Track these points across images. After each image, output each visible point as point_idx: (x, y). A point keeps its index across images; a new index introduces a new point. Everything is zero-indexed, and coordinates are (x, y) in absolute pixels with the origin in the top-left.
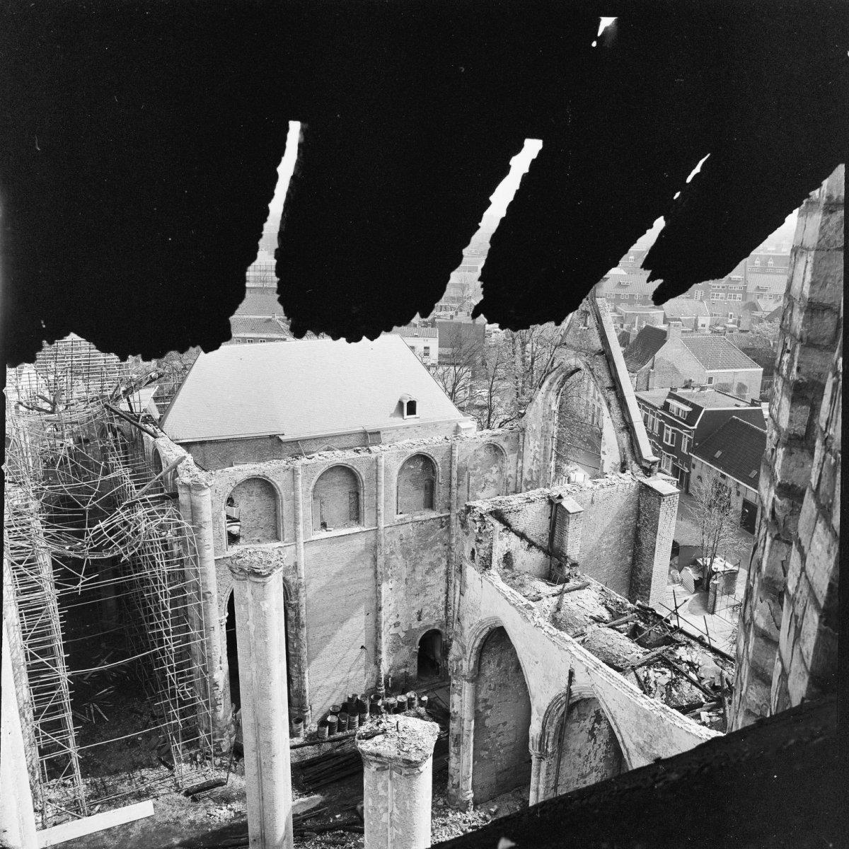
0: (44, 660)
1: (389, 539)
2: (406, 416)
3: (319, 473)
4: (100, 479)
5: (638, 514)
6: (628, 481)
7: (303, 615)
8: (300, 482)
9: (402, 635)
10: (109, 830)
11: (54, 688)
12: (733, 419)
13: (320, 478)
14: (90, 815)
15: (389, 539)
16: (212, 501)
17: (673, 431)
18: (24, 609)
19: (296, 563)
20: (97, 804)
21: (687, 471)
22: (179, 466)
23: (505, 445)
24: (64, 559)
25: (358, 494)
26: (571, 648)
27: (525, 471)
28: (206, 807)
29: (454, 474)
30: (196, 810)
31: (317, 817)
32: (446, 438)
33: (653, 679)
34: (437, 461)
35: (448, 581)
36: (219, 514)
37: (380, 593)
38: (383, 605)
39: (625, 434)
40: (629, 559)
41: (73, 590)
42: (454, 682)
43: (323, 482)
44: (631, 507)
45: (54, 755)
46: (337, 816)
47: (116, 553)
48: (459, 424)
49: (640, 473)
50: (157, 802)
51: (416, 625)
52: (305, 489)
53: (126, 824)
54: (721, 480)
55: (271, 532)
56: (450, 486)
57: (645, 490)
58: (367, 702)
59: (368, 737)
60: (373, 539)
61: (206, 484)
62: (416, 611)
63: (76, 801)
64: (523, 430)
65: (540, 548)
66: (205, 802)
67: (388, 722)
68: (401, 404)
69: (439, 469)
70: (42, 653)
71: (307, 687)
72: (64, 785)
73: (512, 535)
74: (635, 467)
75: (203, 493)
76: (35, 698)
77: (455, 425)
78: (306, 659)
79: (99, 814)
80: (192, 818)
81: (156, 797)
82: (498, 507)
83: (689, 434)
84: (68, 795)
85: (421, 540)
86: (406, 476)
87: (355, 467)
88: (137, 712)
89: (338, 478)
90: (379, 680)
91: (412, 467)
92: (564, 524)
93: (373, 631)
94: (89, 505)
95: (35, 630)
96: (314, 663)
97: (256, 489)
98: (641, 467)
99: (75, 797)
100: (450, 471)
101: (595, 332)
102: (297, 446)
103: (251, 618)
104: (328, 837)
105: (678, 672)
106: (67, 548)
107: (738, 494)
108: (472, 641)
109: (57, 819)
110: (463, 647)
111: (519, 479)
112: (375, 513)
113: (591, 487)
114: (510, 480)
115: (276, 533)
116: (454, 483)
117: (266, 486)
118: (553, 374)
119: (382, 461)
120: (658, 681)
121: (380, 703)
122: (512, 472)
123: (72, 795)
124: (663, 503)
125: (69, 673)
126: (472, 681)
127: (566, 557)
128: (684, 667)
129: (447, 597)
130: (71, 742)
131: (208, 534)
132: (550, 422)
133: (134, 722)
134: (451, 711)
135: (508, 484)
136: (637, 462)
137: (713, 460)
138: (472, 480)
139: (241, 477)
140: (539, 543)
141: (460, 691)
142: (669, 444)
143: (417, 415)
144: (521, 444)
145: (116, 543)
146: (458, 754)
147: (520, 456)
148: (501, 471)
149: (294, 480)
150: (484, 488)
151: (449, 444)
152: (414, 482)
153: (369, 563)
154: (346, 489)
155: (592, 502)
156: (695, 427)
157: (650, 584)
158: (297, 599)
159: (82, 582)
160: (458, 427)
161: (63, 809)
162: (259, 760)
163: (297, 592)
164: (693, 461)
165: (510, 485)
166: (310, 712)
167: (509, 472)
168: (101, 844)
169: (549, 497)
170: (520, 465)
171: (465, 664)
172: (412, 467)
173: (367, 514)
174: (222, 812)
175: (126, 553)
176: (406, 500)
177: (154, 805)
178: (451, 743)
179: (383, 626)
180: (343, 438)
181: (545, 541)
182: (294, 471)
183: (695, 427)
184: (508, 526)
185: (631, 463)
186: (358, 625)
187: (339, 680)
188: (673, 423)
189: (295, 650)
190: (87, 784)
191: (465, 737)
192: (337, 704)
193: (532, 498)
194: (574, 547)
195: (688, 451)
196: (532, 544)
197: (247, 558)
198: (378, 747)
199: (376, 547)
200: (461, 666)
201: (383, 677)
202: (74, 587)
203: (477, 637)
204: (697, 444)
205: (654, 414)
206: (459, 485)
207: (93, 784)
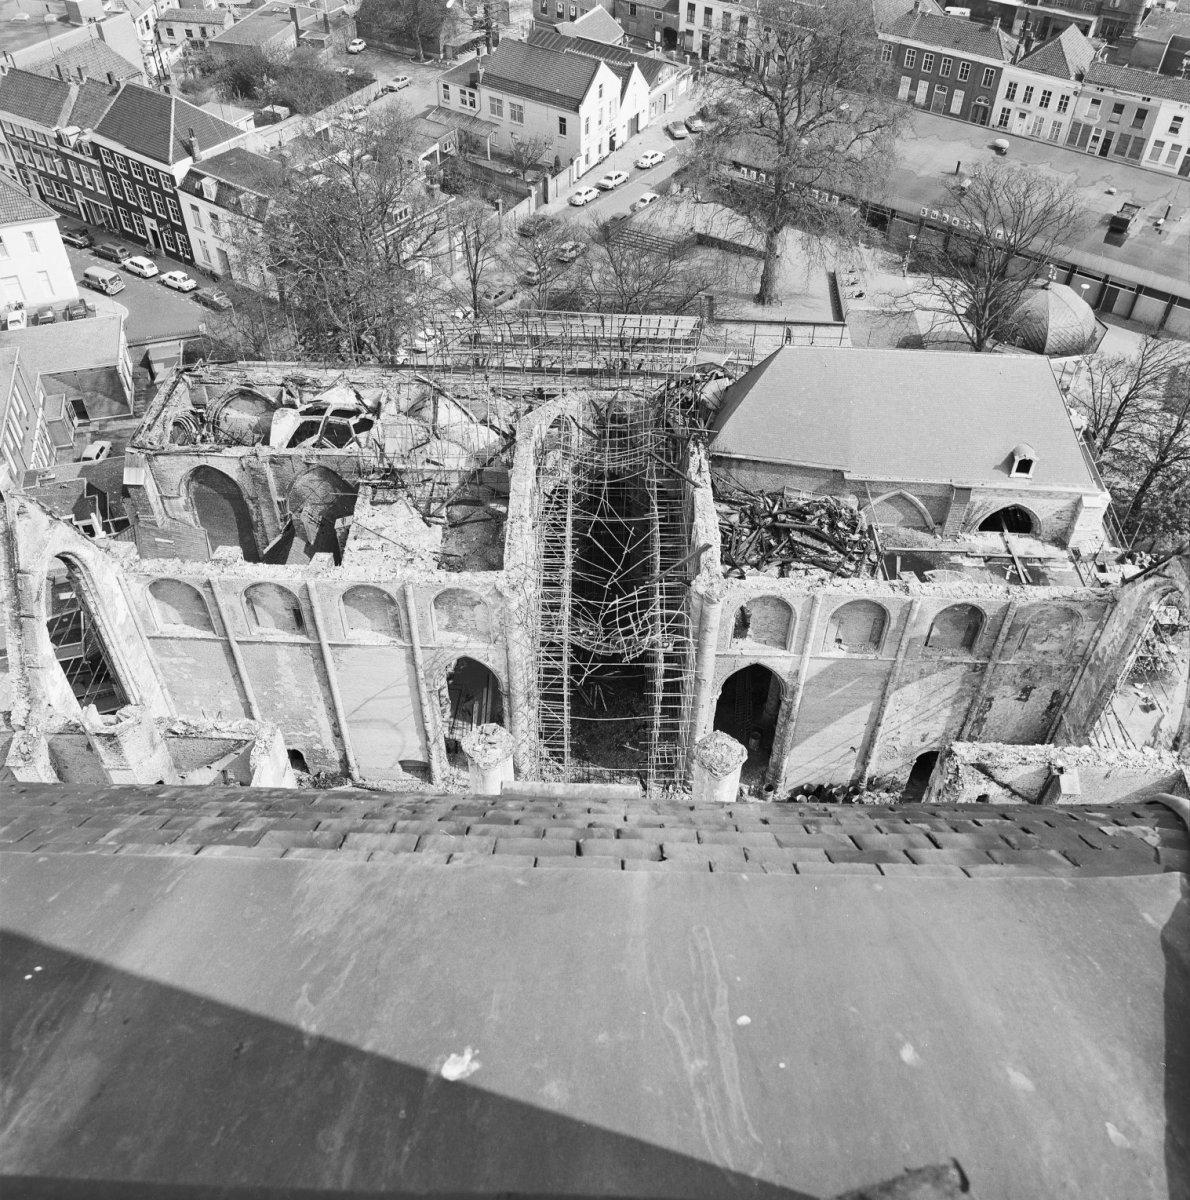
2: (1014, 473)
3: (842, 604)
7: (795, 710)
8: (817, 610)
22: (703, 556)
23: (1084, 612)
29: (1005, 630)
35: (966, 717)
36: (728, 620)
47: (620, 652)
52: (822, 614)
56: (997, 638)
64: (1115, 602)
71: (785, 766)
73: (993, 784)
75: (713, 606)
76: (545, 679)
82: (983, 761)
93: (868, 738)
96: (797, 748)
111: (1091, 647)
113: (1111, 761)
116: (1002, 637)
117: (784, 606)
118: (1162, 580)
119: (917, 607)
122: (1085, 638)
129: (962, 730)
131: (712, 639)
135: (1075, 647)
143: (1030, 475)
147: (1101, 627)
152: (956, 623)
153: (878, 685)
154: (872, 616)
155: (1107, 776)
163: (793, 693)
169: (1050, 763)
170: (1097, 634)
173: (888, 647)
179: (878, 738)
184: (991, 777)
186: (852, 727)
196: (1014, 793)
199: (889, 674)
201: (867, 776)
206: (1008, 639)
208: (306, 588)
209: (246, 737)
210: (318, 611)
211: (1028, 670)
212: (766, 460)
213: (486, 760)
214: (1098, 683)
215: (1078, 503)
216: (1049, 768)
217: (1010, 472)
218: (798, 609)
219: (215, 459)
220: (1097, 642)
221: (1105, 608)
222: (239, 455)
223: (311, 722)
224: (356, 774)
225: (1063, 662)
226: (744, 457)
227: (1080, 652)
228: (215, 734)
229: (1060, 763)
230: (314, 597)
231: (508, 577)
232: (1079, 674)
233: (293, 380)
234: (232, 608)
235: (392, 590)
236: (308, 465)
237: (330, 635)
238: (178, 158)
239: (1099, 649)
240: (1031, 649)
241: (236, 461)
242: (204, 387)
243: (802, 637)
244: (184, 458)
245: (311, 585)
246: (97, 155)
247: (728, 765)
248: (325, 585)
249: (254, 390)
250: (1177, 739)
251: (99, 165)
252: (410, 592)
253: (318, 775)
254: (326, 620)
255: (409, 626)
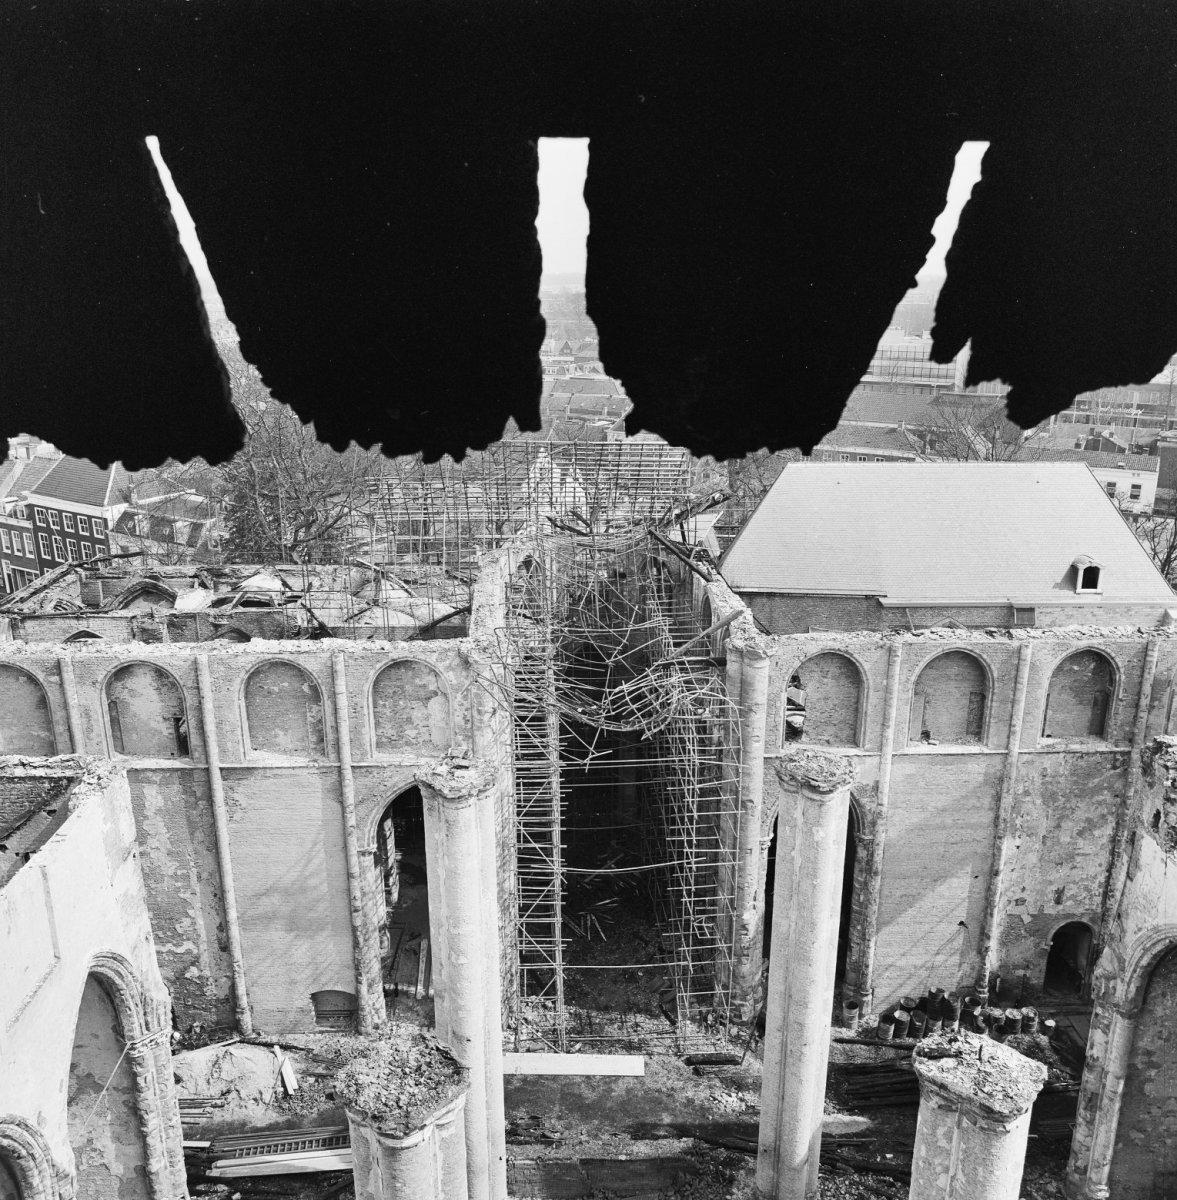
0: (537, 846)
1: (1023, 771)
2: (1079, 589)
3: (928, 659)
4: (630, 628)
7: (878, 857)
8: (897, 669)
9: (1027, 919)
10: (588, 1077)
11: (546, 883)
13: (929, 666)
14: (568, 1052)
15: (1023, 771)
16: (770, 677)
18: (524, 778)
19: (877, 782)
20: (577, 1042)
22: (732, 623)
24: (576, 725)
25: (983, 697)
28: (710, 1087)
29: (1147, 689)
30: (697, 1085)
31: (860, 1147)
32: (1139, 631)
34: (1120, 664)
35: (1113, 853)
36: (778, 695)
37: (999, 849)
38: (1001, 867)
41: (578, 765)
42: (1099, 1010)
43: (932, 673)
45: (535, 966)
46: (889, 1156)
47: (636, 727)
50: (649, 1061)
51: (1051, 909)
52: (903, 678)
53: (609, 1077)
55: (847, 732)
56: (1137, 706)
58: (958, 1005)
59: (935, 1055)
60: (999, 767)
61: (765, 653)
62: (1054, 888)
63: (555, 1030)
66: (710, 1079)
67: (967, 1042)
68: (1074, 569)
69: (1121, 677)
70: (538, 837)
71: (871, 962)
72: (545, 1007)
75: (759, 664)
76: (524, 891)
78: (874, 922)
79: (580, 1055)
80: (690, 1094)
81: (650, 1055)
84: (547, 1020)
85: (1076, 782)
86: (1066, 681)
87: (985, 656)
88: (641, 939)
89: (954, 669)
90: (980, 978)
91: (1076, 668)
93: (983, 903)
94: (612, 659)
95: (531, 807)
96: (886, 930)
97: (833, 668)
99: (554, 1025)
100: (1141, 683)
102: (904, 615)
103: (797, 848)
104: (870, 1180)
106: (580, 710)
108: (1138, 955)
109: (532, 1045)
110: (1121, 961)
112: (1007, 728)
115: (855, 735)
116: (1145, 702)
117: (849, 668)
119: (1027, 653)
121: (977, 1011)
123: (552, 1022)
125: (565, 870)
126: (1128, 1016)
129: (1109, 878)
130: (559, 956)
131: (759, 721)
133: (636, 951)
134: (1089, 1053)
139: (813, 649)
141: (1108, 1027)
143: (1098, 590)
145: (639, 714)
146: (1090, 1123)
149: (890, 664)
151: (1144, 641)
152: (1077, 691)
153: (987, 801)
154: (967, 687)
158: (873, 833)
159: (590, 756)
161: (539, 1034)
162: (784, 1045)
163: (874, 824)
166: (870, 997)
168: (576, 1091)
171: (1121, 989)
172: (1076, 668)
174: (729, 1099)
175: (649, 729)
176: (1060, 717)
177: (646, 1064)
178: (1082, 1104)
179: (997, 899)
180: (975, 612)
182: (891, 651)
186: (957, 892)
187: (919, 963)
189: (861, 904)
190: (570, 1014)
191: (1106, 1101)
192: (912, 996)
197: (802, 763)
198: (945, 1075)
199: (1001, 780)
200: (1114, 988)
201: (987, 974)
202: (580, 762)
203: (1146, 950)
206: (1151, 707)
207: (577, 1016)
208: (195, 667)
209: (69, 773)
210: (209, 706)
212: (782, 591)
213: (453, 784)
217: (1074, 587)
218: (868, 663)
219: (98, 621)
222: (131, 615)
223: (186, 922)
224: (247, 1020)
226: (756, 590)
228: (19, 772)
230: (206, 681)
231: (477, 641)
233: (208, 570)
234: (86, 713)
235: (311, 665)
236: (217, 626)
237: (223, 751)
238: (113, 503)
241: (124, 623)
242: (99, 582)
243: (880, 719)
244: (59, 622)
245: (203, 659)
246: (31, 517)
247: (833, 775)
248: (221, 661)
249: (161, 584)
251: (31, 526)
252: (340, 667)
253: (189, 1031)
254: (219, 724)
255: (336, 729)
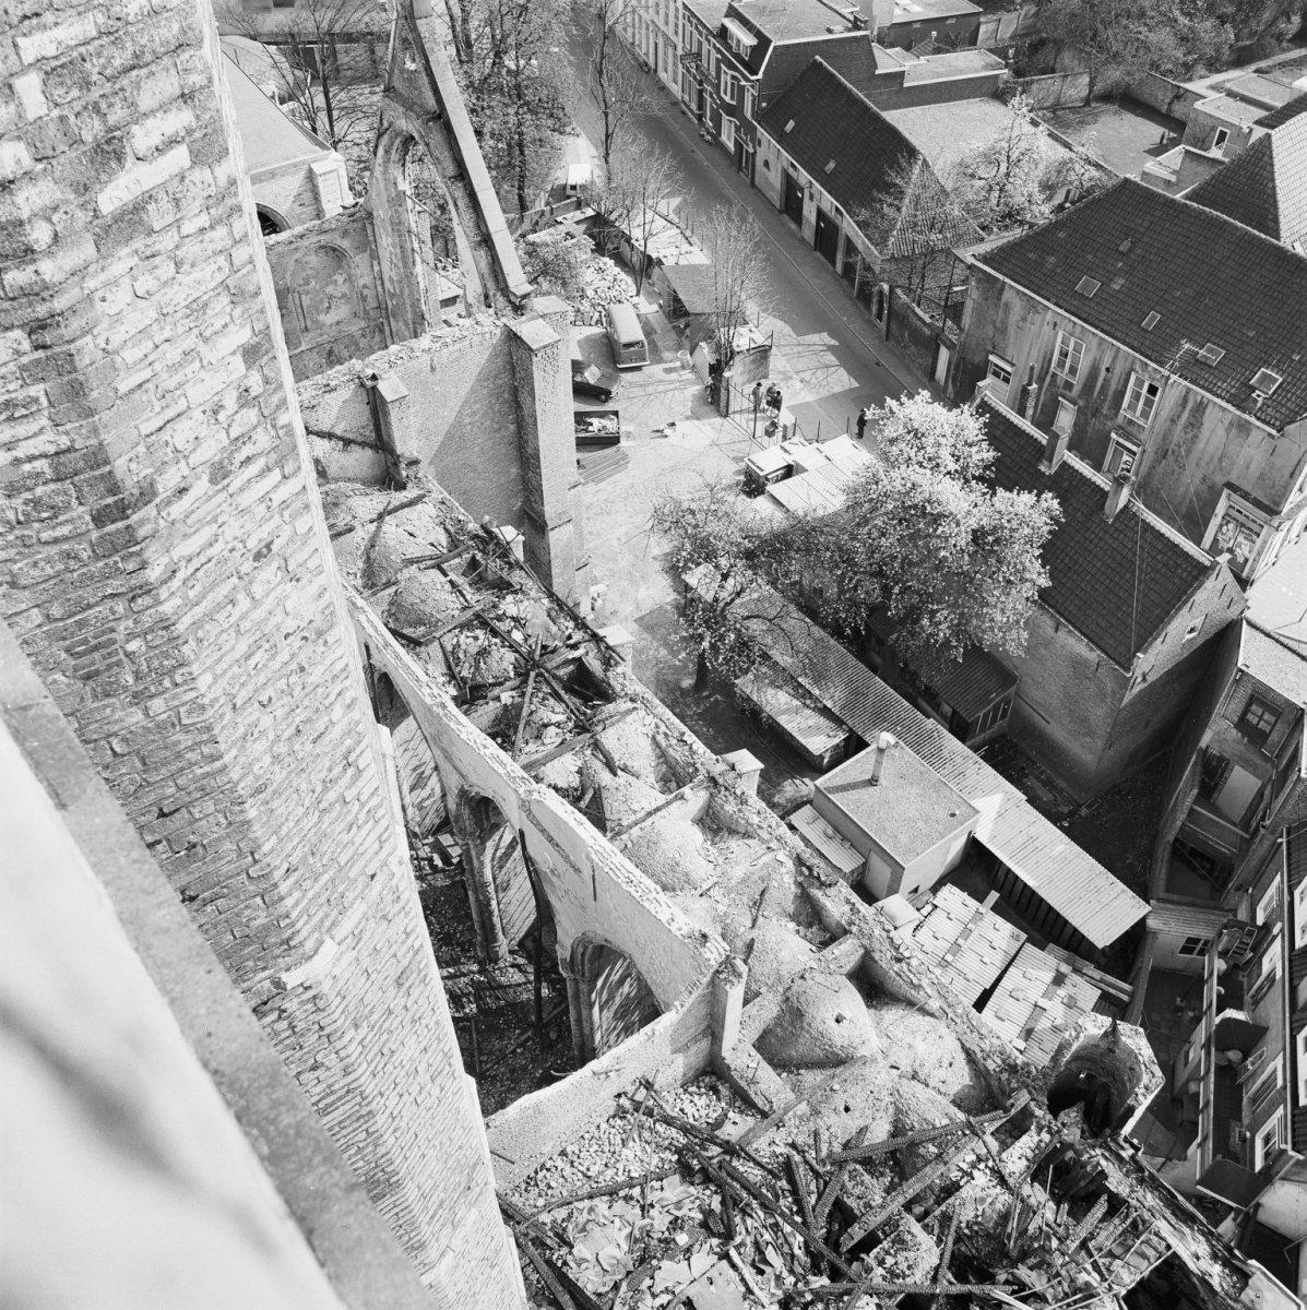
5: (512, 368)
6: (488, 326)
12: (815, 61)
17: (733, 77)
21: (751, 150)
23: (345, 244)
26: (362, 618)
27: (386, 278)
33: (463, 647)
39: (483, 252)
40: (512, 427)
44: (500, 362)
48: (313, 166)
49: (508, 311)
54: (791, 170)
57: (512, 337)
64: (370, 215)
65: (363, 444)
74: (501, 301)
77: (306, 166)
83: (753, 87)
92: (387, 414)
98: (510, 302)
101: (424, 80)
105: (495, 633)
107: (811, 197)
111: (380, 289)
114: (366, 292)
120: (470, 649)
122: (367, 280)
124: (535, 359)
127: (398, 456)
128: (503, 626)
132: (400, 210)
135: (364, 299)
136: (503, 295)
137: (782, 138)
138: (306, 301)
140: (360, 439)
142: (727, 99)
144: (371, 238)
148: (349, 280)
150: (329, 307)
155: (433, 369)
156: (760, 76)
157: (539, 461)
160: (311, 171)
164: (759, 135)
165: (369, 299)
167: (361, 282)
169: (359, 378)
170: (376, 268)
181: (370, 435)
183: (760, 76)
185: (495, 295)
188: (731, 66)
193: (333, 384)
194: (408, 440)
195: (753, 116)
204: (764, 105)
205: (709, 41)
211: (330, 353)
214: (406, 324)
215: (311, 176)
216: (362, 385)
220: (381, 279)
221: (364, 228)
225: (363, 324)
227: (372, 303)
229: (369, 372)
232: (387, 332)
239: (388, 285)
240: (320, 326)
250: (486, 297)
